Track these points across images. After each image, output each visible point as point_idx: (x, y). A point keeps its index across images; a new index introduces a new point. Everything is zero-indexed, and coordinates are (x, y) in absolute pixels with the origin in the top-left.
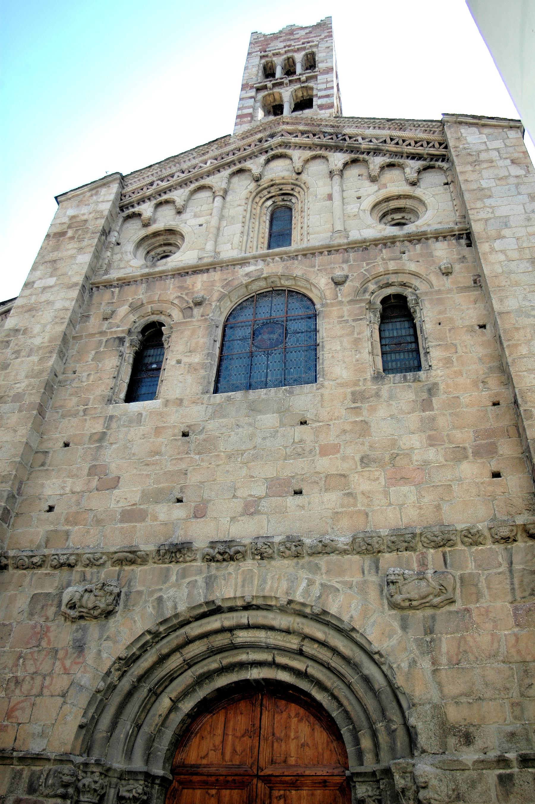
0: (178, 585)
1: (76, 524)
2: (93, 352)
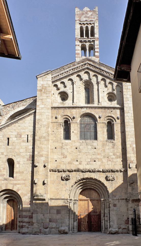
1: (61, 164)
2: (56, 127)
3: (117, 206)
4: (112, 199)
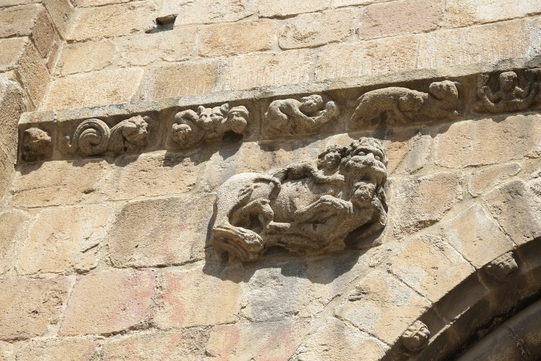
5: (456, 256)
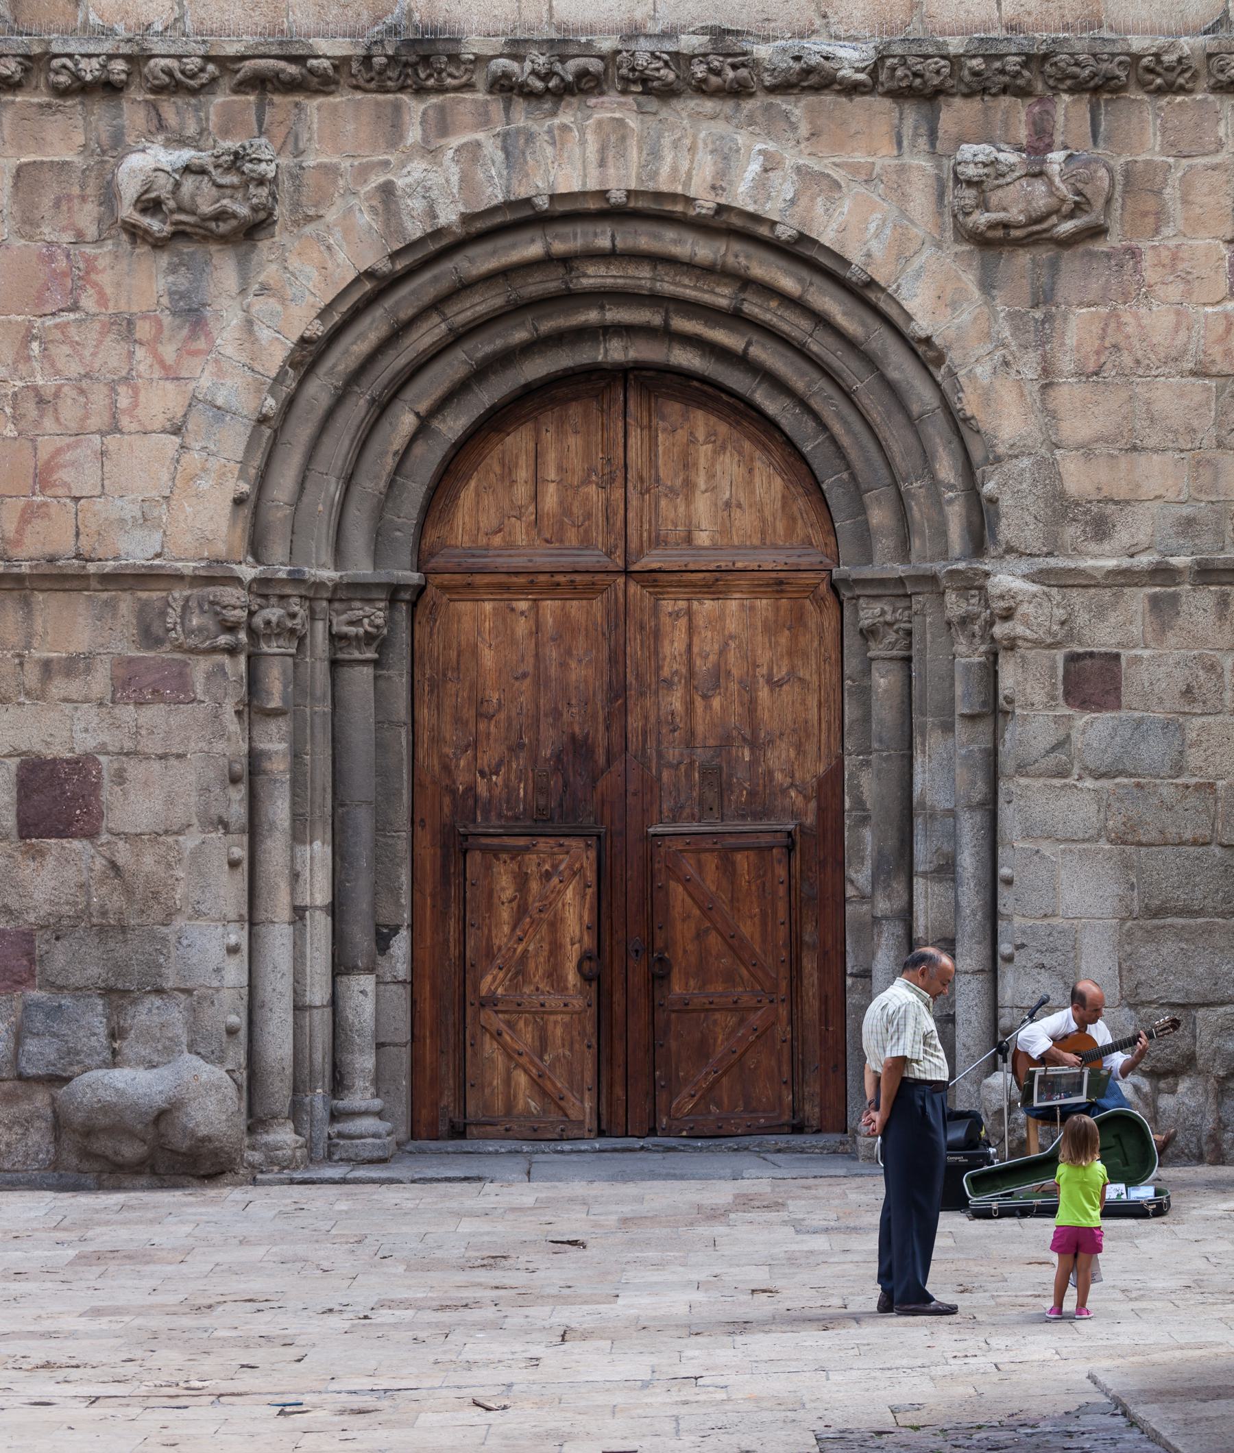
0: (430, 152)
3: (1134, 680)
4: (1043, 563)
5: (341, 256)
